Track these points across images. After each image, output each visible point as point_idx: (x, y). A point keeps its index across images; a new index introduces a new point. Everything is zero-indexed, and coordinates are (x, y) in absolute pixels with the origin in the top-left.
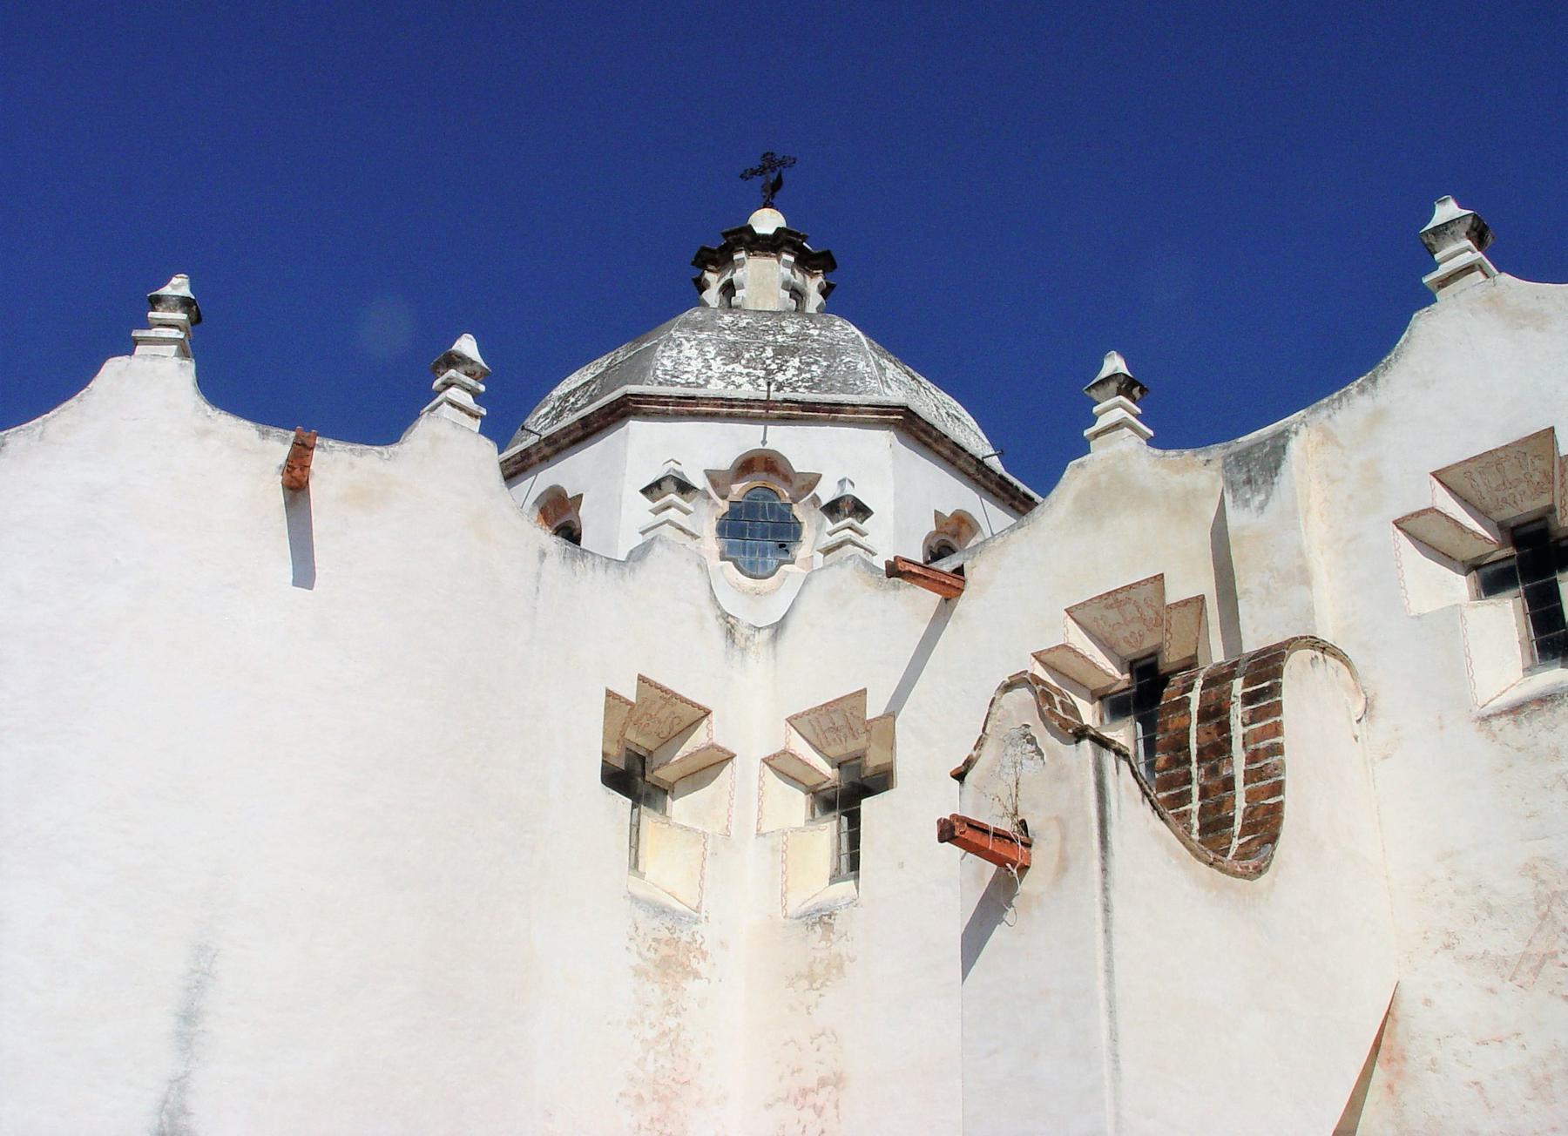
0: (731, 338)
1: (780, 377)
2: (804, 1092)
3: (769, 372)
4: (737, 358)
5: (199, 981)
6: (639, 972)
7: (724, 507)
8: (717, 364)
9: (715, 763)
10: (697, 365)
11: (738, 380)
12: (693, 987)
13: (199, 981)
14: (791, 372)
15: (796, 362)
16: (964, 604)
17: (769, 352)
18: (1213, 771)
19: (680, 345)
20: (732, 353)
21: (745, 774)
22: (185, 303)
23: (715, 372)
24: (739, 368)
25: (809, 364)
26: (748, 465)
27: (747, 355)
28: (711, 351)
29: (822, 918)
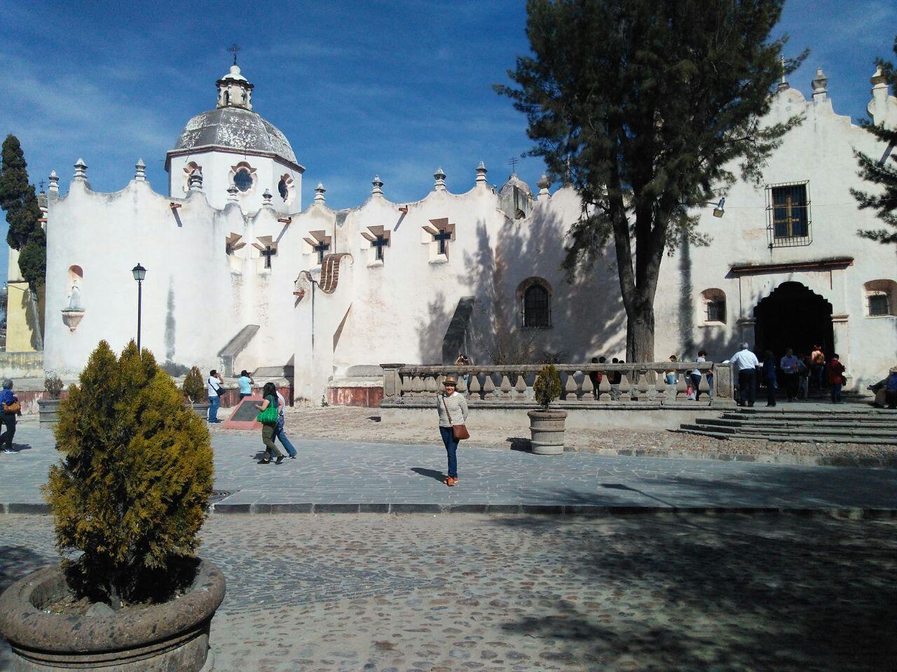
1: (247, 141)
2: (261, 305)
5: (171, 296)
6: (233, 286)
7: (235, 173)
8: (232, 135)
9: (243, 245)
10: (227, 136)
12: (241, 287)
13: (171, 296)
15: (250, 136)
16: (291, 225)
17: (243, 133)
18: (329, 274)
20: (235, 132)
21: (248, 247)
22: (144, 168)
26: (240, 164)
29: (264, 276)
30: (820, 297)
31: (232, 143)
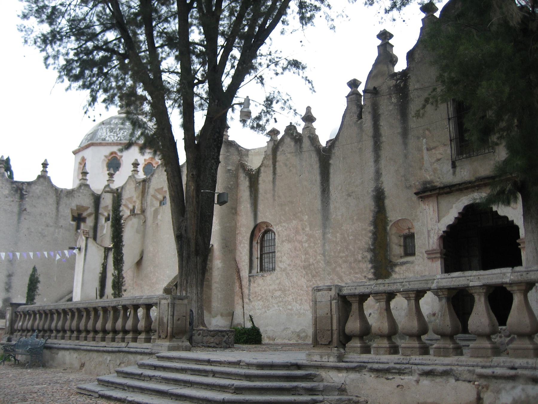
0: (112, 126)
1: (119, 135)
3: (117, 134)
4: (111, 132)
8: (109, 134)
10: (105, 134)
11: (112, 137)
14: (121, 134)
15: (122, 132)
19: (103, 129)
20: (111, 130)
23: (107, 136)
24: (112, 134)
25: (124, 132)
26: (112, 153)
27: (114, 131)
28: (108, 130)
30: (506, 218)
31: (107, 138)
